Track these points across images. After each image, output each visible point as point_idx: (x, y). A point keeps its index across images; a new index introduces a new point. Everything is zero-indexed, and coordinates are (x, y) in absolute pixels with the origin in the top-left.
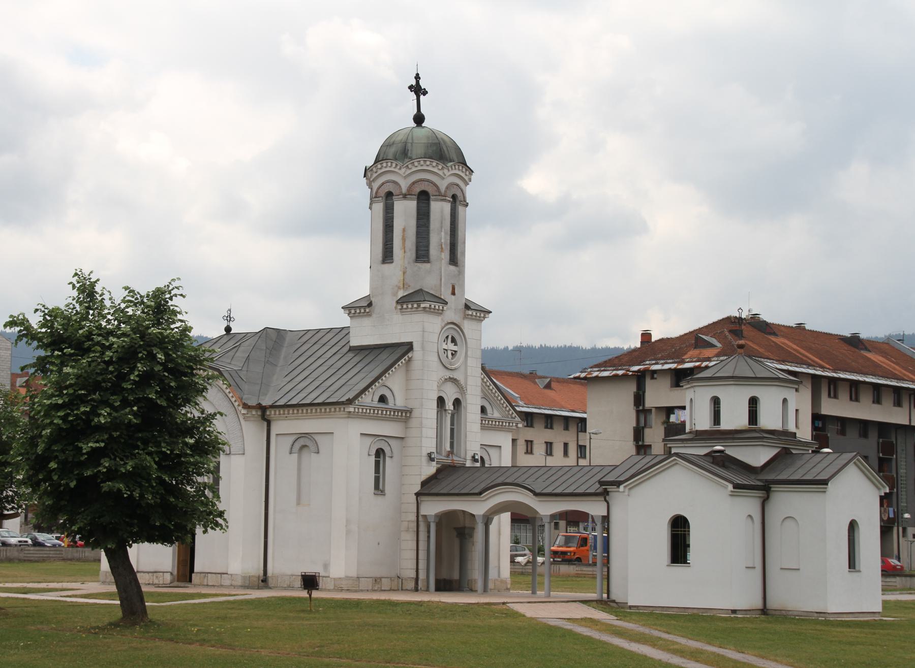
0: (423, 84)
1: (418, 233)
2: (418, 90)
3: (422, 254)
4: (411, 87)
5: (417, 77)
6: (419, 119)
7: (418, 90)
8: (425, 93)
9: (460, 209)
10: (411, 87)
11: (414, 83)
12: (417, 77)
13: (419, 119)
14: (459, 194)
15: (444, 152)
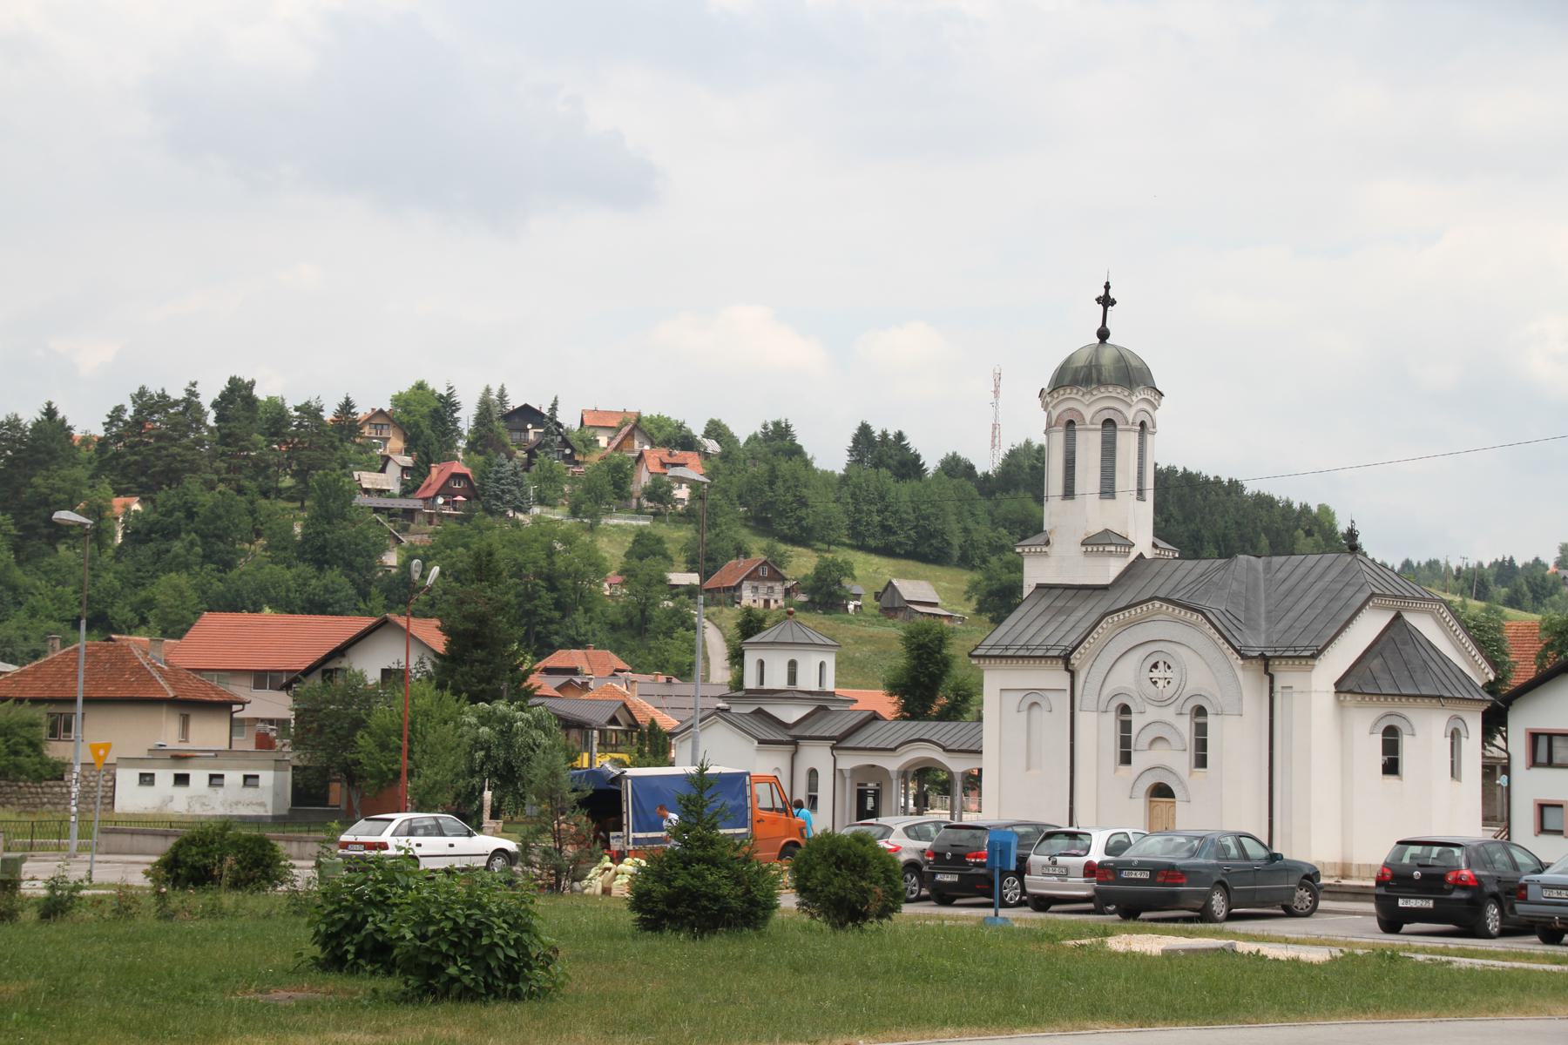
0: (1112, 294)
1: (1103, 469)
2: (1106, 301)
3: (1108, 490)
4: (1098, 300)
5: (1107, 287)
6: (1103, 334)
7: (1106, 301)
8: (1113, 303)
9: (1149, 437)
10: (1098, 300)
11: (1102, 293)
12: (1107, 287)
13: (1103, 334)
14: (1149, 424)
15: (1132, 375)
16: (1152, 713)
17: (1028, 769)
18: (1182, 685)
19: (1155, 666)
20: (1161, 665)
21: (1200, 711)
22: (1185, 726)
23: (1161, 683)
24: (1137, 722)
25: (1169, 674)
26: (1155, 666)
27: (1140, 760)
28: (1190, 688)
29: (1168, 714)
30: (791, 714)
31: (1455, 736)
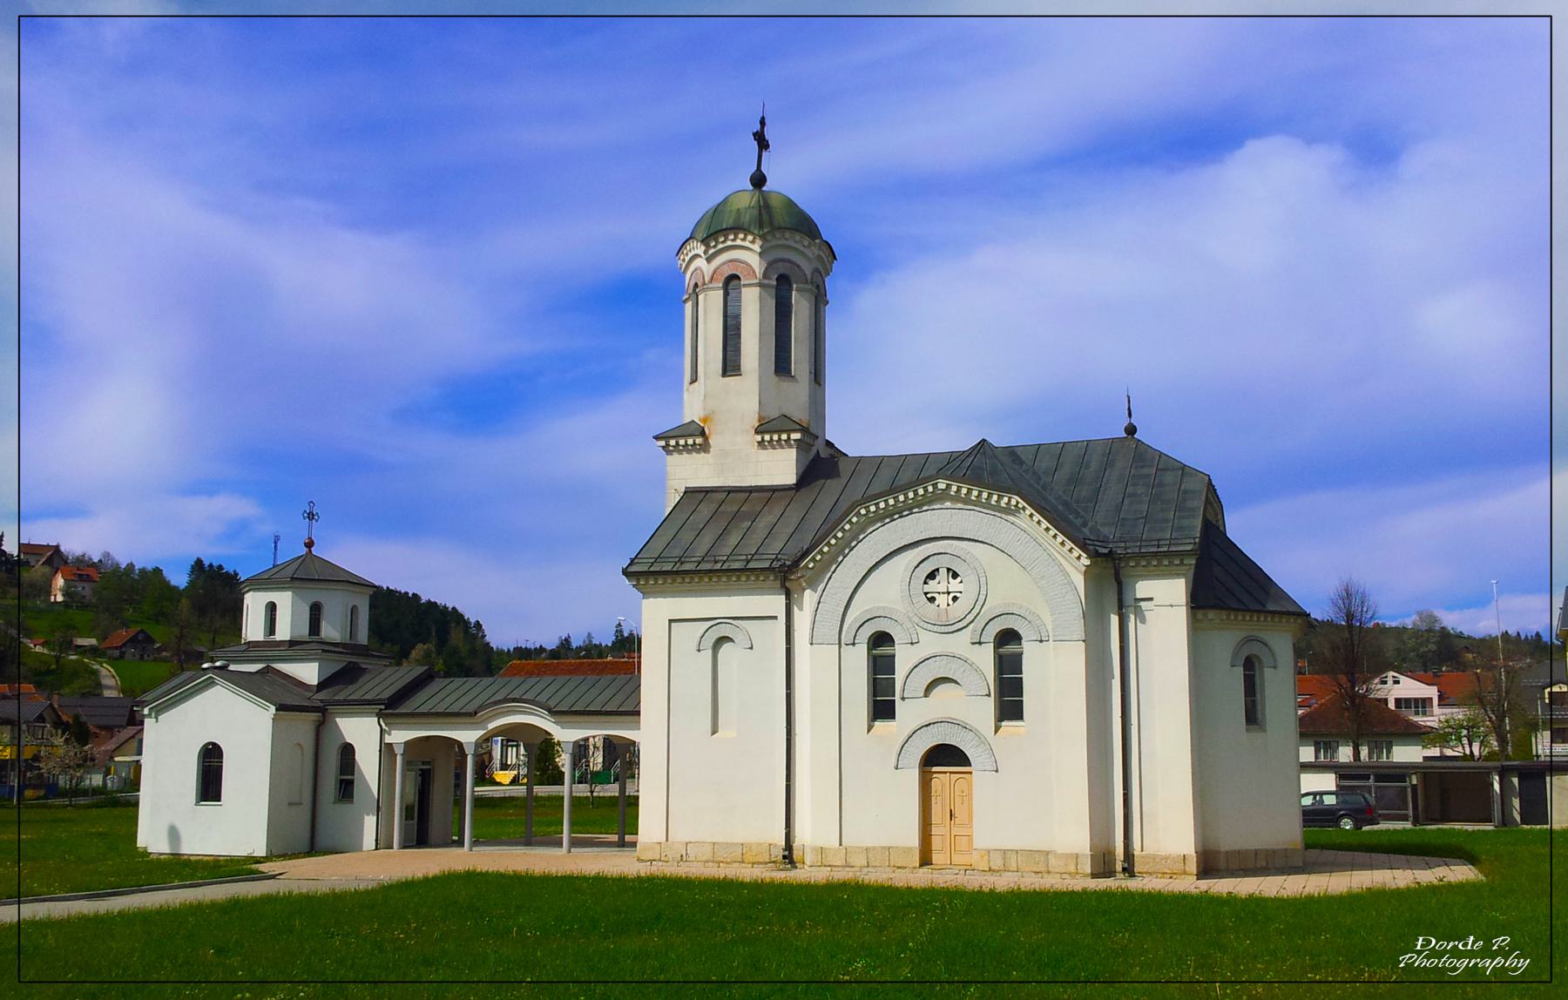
5: (763, 122)
7: (762, 142)
12: (763, 122)
16: (931, 643)
17: (714, 732)
18: (980, 601)
19: (932, 575)
20: (943, 572)
21: (1008, 637)
22: (985, 658)
23: (942, 600)
24: (904, 658)
25: (954, 585)
26: (932, 575)
27: (910, 712)
28: (993, 605)
29: (960, 643)
30: (308, 672)
31: (1251, 667)
